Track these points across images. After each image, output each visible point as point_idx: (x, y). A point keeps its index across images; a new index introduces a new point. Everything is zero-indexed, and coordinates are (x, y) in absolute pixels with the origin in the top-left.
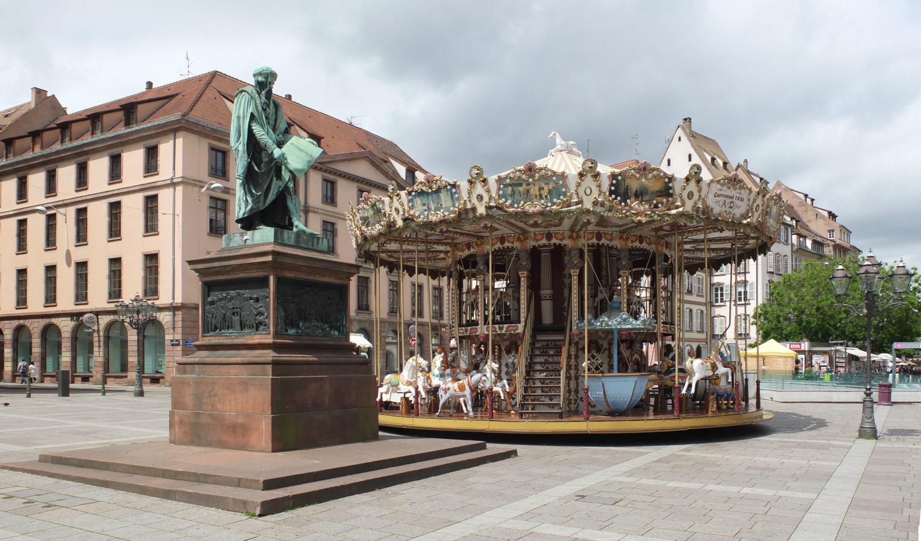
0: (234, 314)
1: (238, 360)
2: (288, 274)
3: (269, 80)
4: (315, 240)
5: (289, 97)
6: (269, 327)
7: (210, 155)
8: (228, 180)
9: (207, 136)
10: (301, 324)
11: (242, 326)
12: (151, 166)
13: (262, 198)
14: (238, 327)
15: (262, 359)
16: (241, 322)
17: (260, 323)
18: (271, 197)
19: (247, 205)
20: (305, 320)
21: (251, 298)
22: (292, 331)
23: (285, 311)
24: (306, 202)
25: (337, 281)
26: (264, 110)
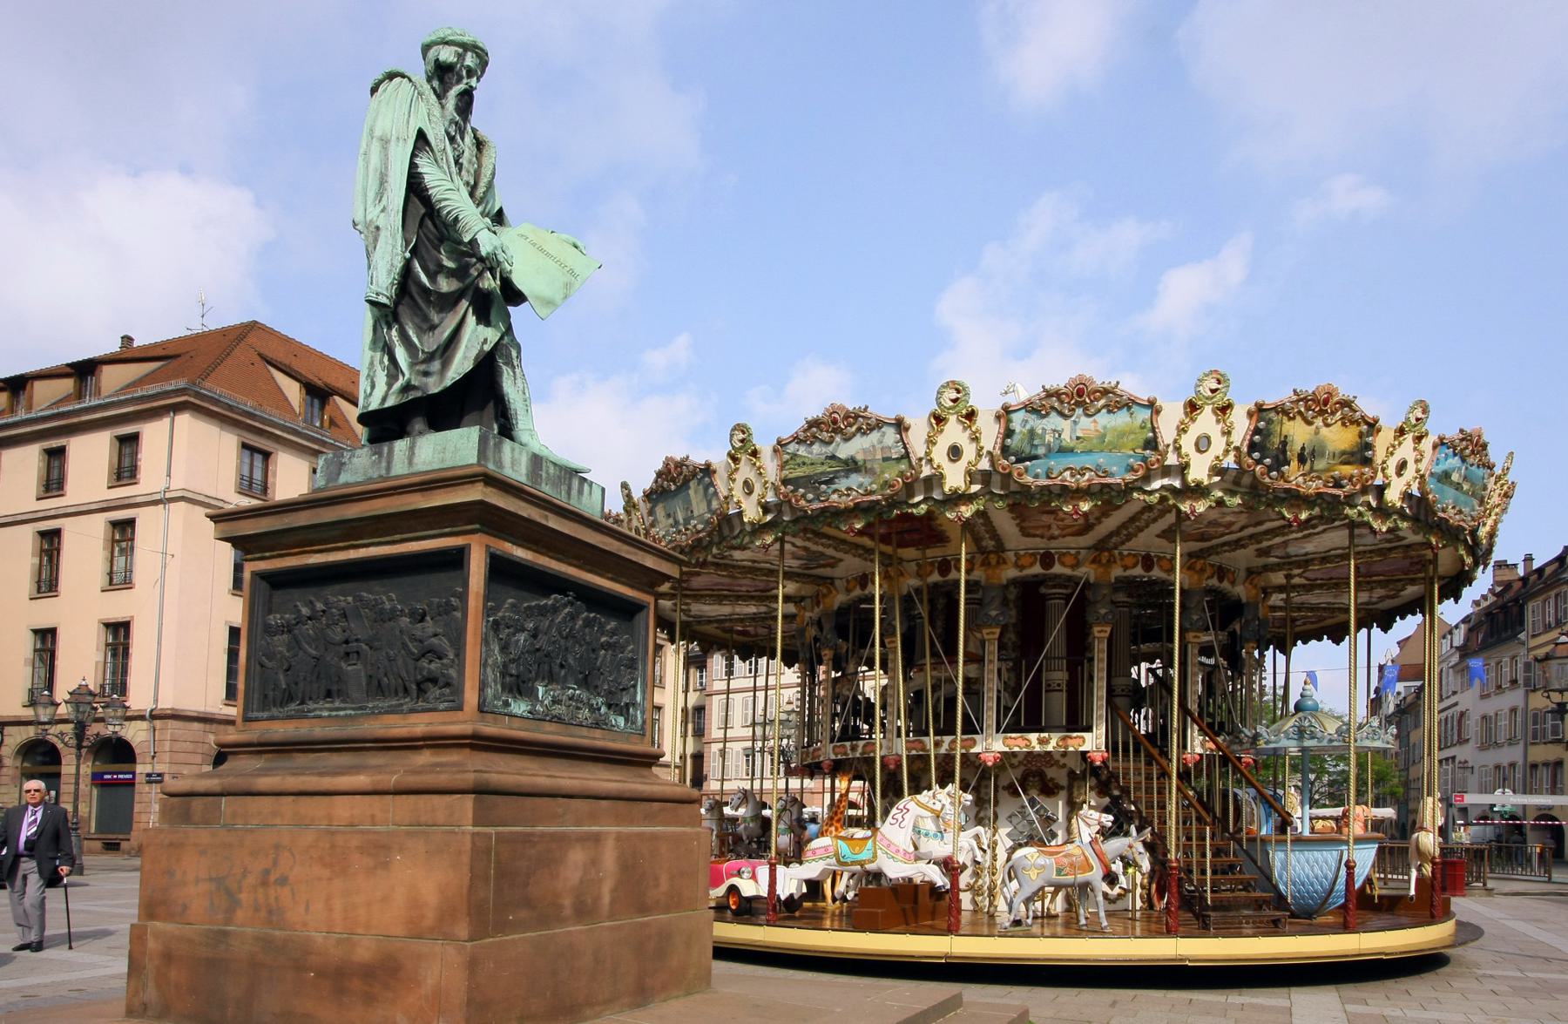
7: (240, 458)
12: (125, 471)
15: (443, 779)
18: (462, 363)
20: (551, 678)
22: (520, 707)
23: (504, 648)
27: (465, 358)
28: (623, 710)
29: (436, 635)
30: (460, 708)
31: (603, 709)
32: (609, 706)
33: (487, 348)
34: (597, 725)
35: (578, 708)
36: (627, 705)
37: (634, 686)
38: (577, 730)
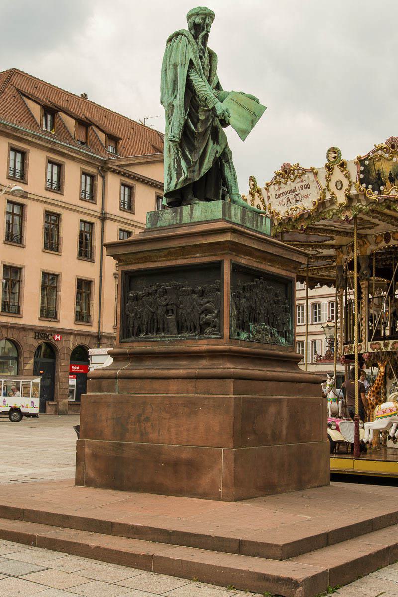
0: (167, 312)
1: (182, 372)
2: (243, 261)
3: (207, 22)
4: (259, 219)
5: (85, 96)
6: (220, 330)
8: (26, 183)
9: (8, 135)
10: (251, 327)
11: (180, 329)
13: (197, 166)
14: (173, 329)
16: (178, 322)
17: (208, 324)
18: (208, 164)
19: (179, 174)
20: (255, 321)
21: (193, 292)
22: (244, 336)
23: (237, 308)
24: (103, 209)
25: (284, 273)
26: (201, 58)
27: (209, 161)
28: (283, 335)
29: (208, 302)
30: (222, 338)
31: (276, 335)
32: (278, 333)
33: (218, 155)
34: (274, 343)
35: (266, 335)
36: (285, 332)
37: (288, 322)
38: (266, 346)
